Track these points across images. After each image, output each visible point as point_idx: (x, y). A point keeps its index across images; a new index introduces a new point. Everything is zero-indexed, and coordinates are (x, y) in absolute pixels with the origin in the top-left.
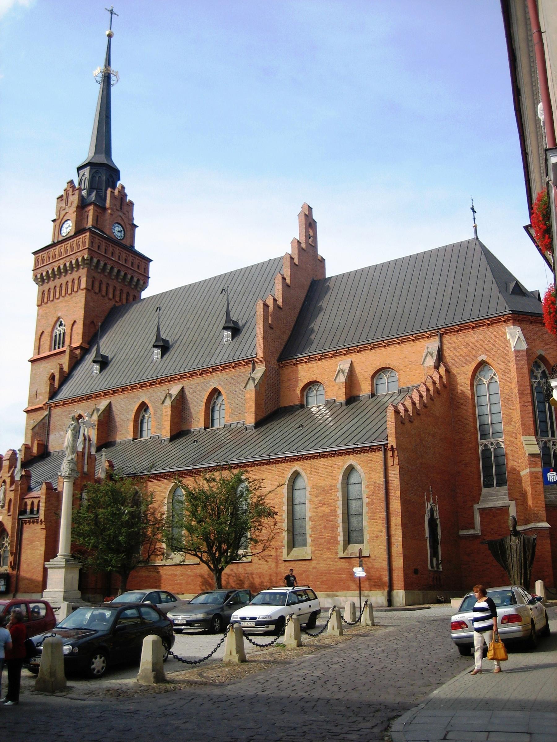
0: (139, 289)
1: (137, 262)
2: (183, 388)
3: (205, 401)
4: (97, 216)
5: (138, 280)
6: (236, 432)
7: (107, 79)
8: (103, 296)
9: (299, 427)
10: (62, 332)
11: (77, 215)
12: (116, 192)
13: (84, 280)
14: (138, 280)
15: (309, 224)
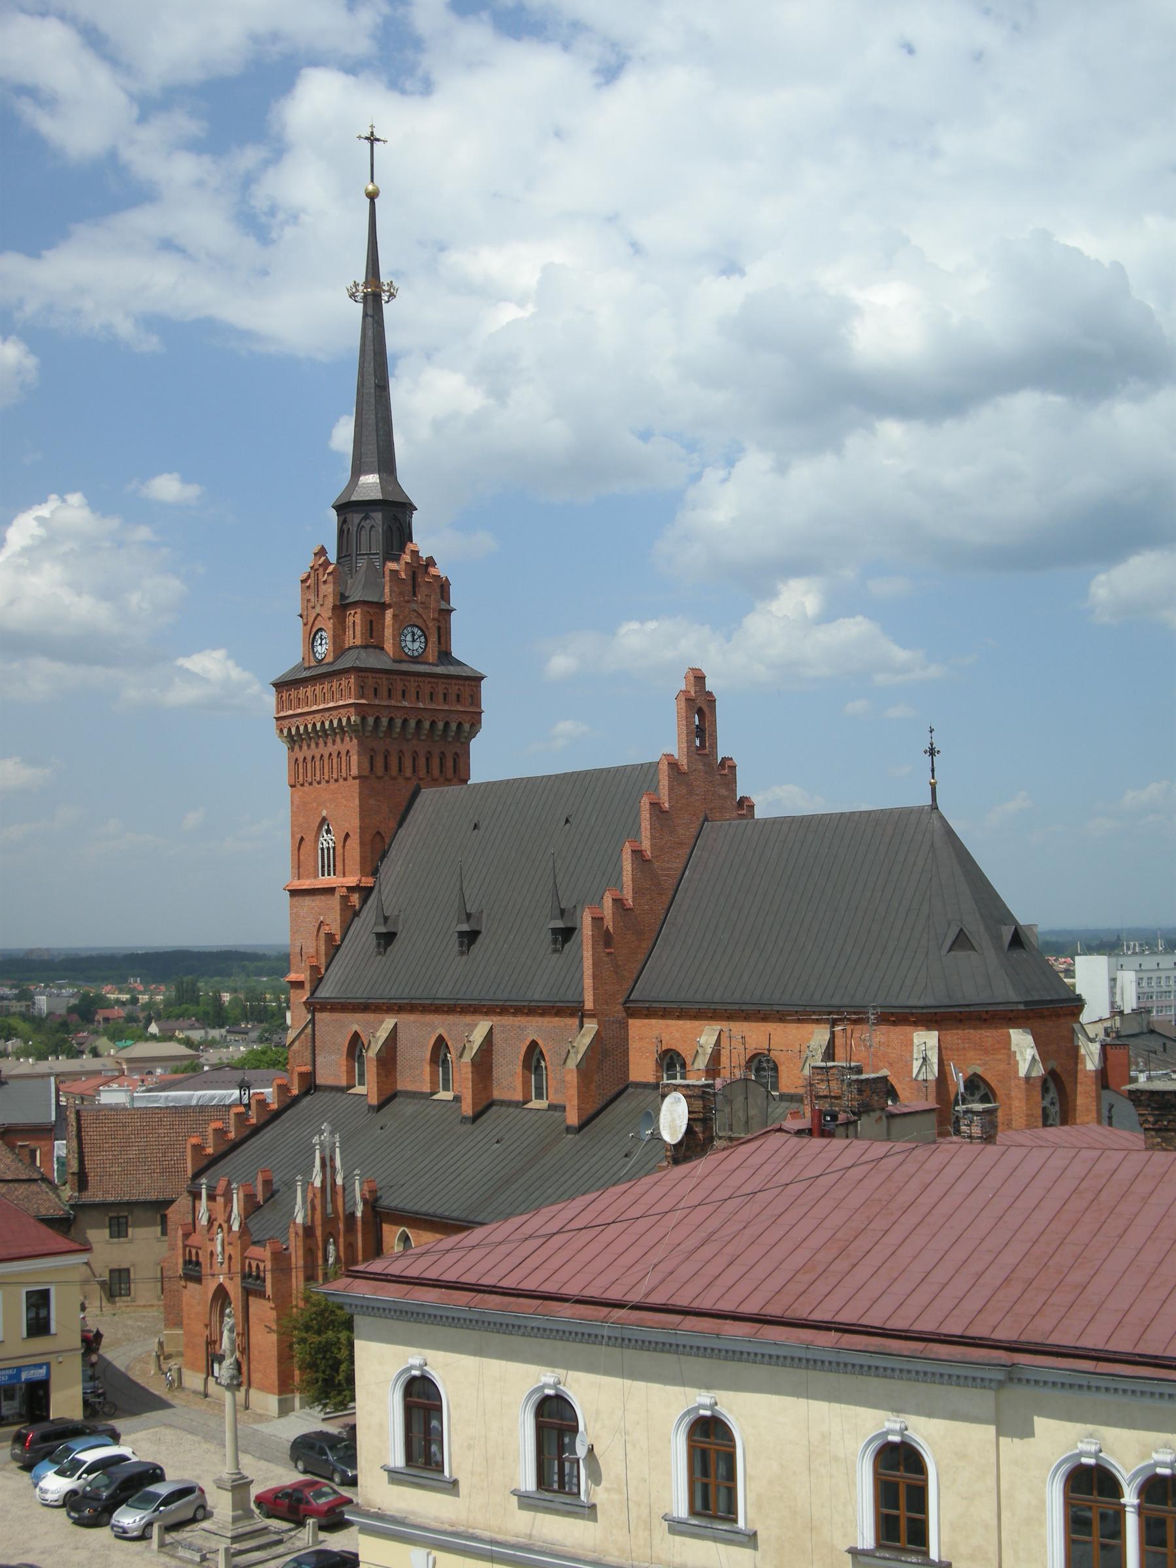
0: (463, 740)
1: (454, 690)
2: (491, 1028)
3: (522, 1058)
4: (371, 622)
5: (460, 725)
8: (394, 779)
9: (626, 1156)
10: (331, 845)
11: (334, 625)
13: (354, 758)
14: (460, 725)
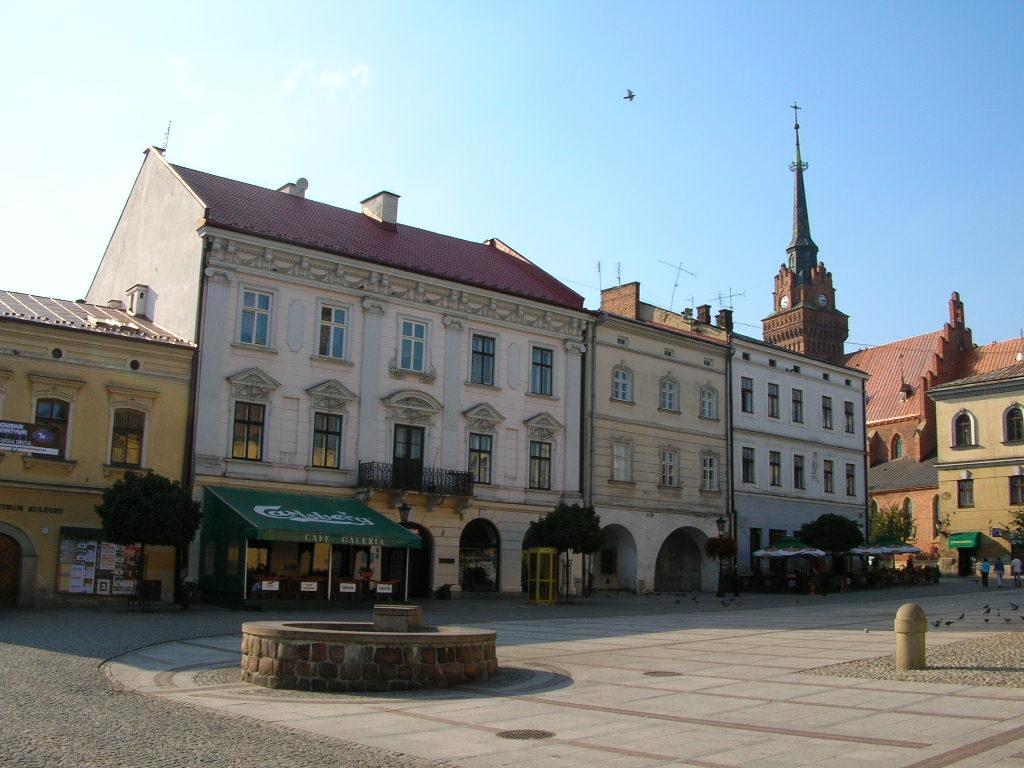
6: (907, 463)
7: (800, 169)
12: (818, 269)
13: (802, 344)
15: (957, 305)
